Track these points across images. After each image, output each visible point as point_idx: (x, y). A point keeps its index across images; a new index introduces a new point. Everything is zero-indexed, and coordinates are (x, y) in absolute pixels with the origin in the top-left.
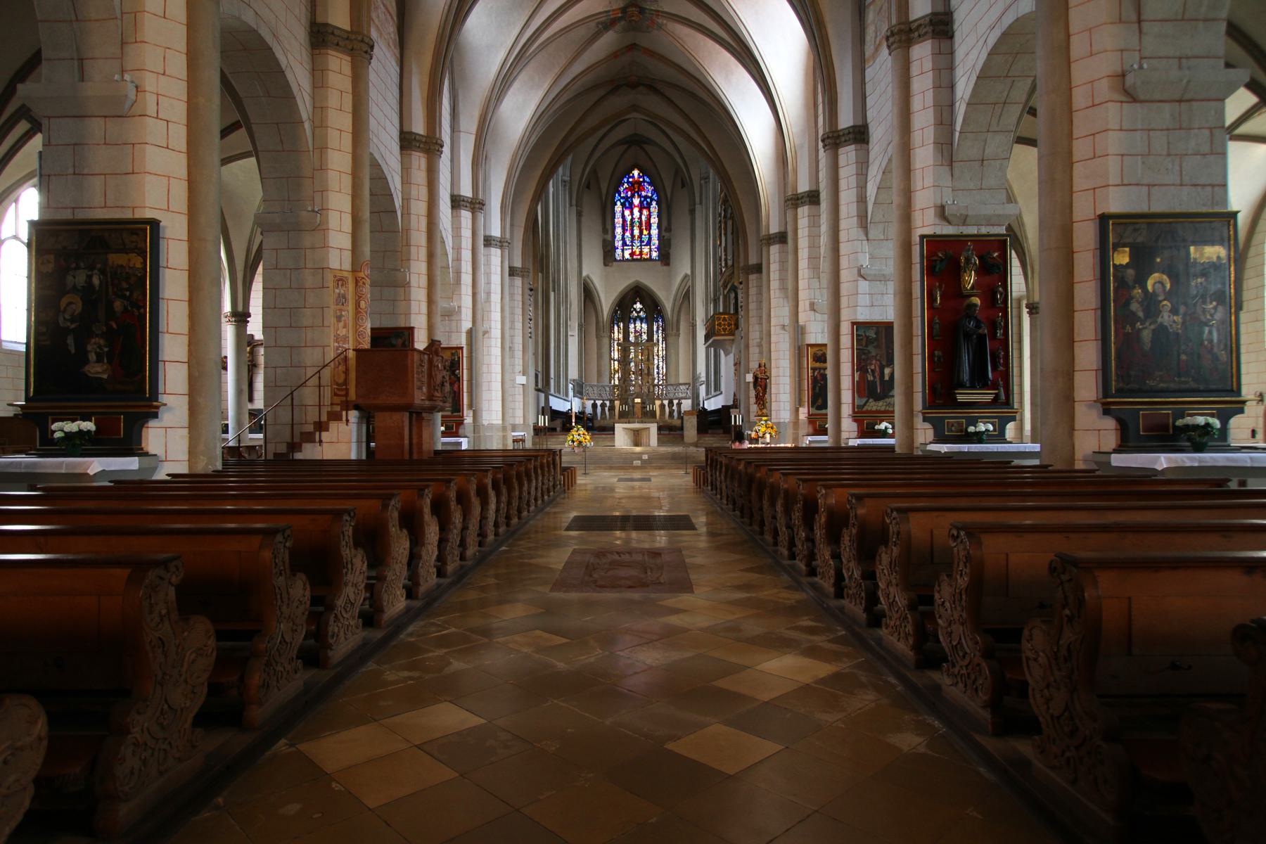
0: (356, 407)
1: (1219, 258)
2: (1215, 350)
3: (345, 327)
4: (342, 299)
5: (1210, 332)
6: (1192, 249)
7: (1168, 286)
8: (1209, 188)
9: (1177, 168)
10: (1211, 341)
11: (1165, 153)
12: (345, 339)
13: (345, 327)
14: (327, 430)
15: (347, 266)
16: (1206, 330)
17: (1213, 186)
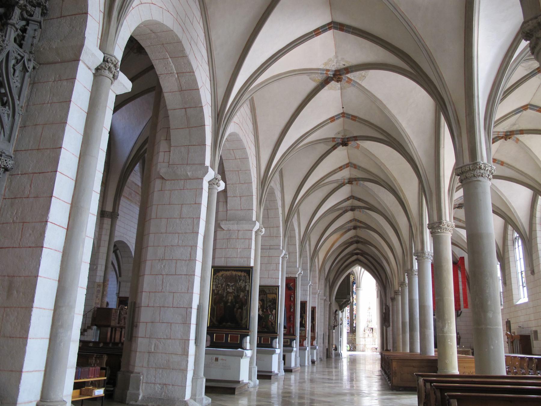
0: (96, 325)
1: (274, 297)
2: (272, 321)
3: (98, 300)
4: (98, 291)
5: (271, 317)
6: (268, 295)
7: (261, 304)
8: (275, 279)
9: (268, 273)
10: (271, 319)
11: (265, 270)
12: (98, 304)
13: (98, 300)
14: (86, 332)
15: (102, 281)
16: (270, 316)
17: (276, 278)
